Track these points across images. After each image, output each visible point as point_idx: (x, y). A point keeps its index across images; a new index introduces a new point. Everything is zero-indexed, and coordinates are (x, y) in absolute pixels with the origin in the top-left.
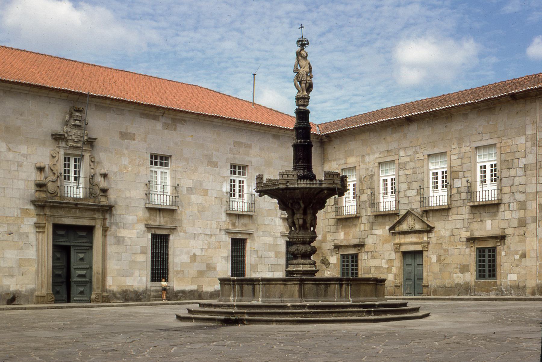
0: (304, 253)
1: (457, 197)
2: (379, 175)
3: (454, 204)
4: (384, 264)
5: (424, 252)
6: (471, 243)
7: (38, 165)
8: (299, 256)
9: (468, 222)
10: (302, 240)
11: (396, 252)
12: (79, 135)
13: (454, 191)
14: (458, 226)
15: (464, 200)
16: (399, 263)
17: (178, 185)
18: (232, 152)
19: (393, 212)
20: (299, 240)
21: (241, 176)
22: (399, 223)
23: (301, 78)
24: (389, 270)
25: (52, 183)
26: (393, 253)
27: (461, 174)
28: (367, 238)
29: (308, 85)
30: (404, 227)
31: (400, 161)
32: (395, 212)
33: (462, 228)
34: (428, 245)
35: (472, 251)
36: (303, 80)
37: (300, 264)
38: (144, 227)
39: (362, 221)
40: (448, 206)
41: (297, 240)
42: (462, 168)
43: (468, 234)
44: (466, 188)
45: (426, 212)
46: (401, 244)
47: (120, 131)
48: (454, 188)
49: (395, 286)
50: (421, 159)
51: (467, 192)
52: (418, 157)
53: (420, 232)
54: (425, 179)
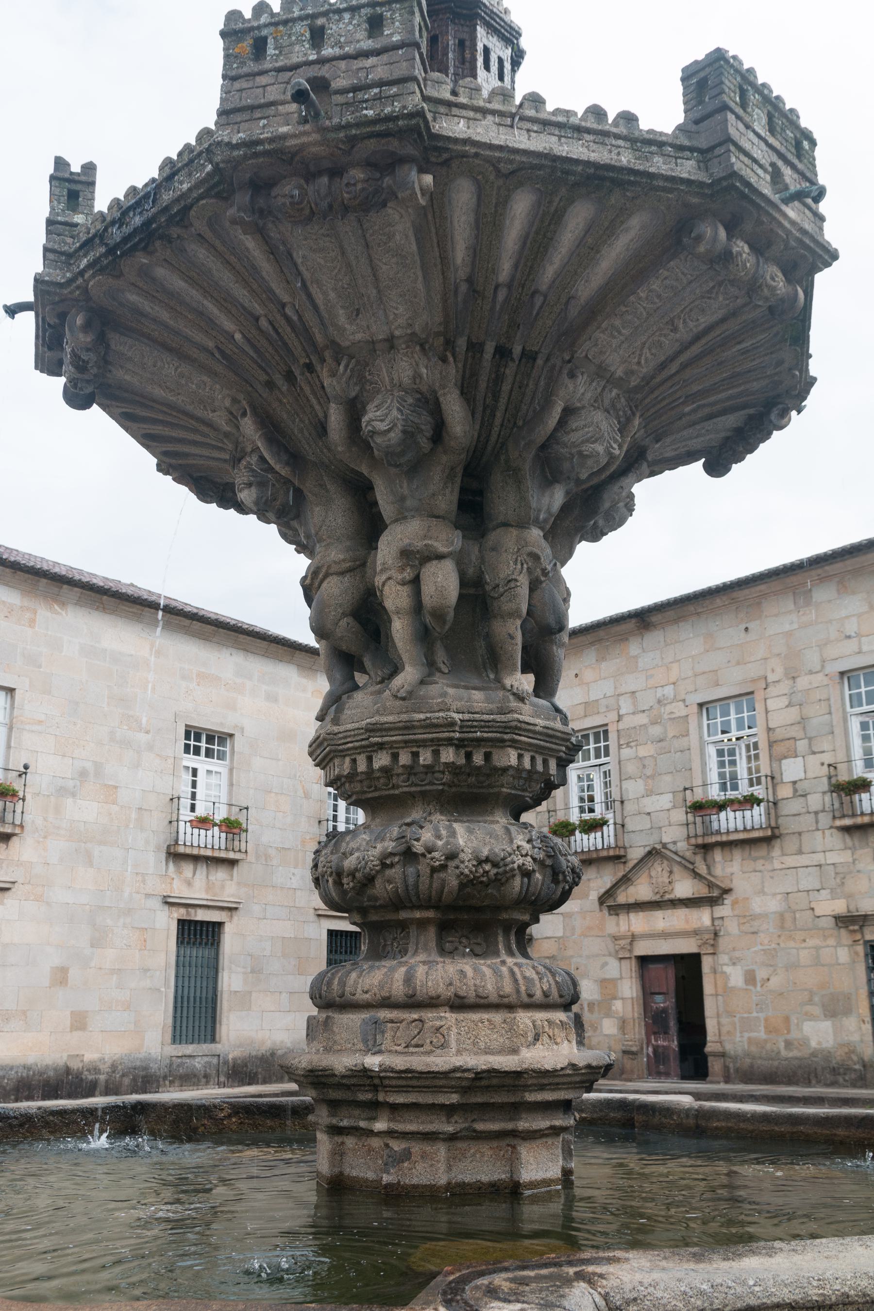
0: (468, 883)
3: (788, 825)
6: (854, 931)
8: (422, 924)
9: (837, 873)
10: (448, 755)
11: (621, 959)
13: (784, 792)
14: (804, 885)
15: (816, 813)
16: (631, 988)
17: (26, 767)
19: (611, 853)
20: (425, 757)
22: (625, 880)
27: (802, 745)
30: (641, 890)
31: (621, 726)
32: (617, 853)
33: (818, 891)
35: (856, 953)
37: (433, 1003)
40: (772, 831)
41: (405, 759)
43: (840, 907)
44: (825, 780)
46: (633, 938)
48: (782, 782)
49: (624, 1052)
50: (680, 717)
51: (824, 793)
52: (672, 713)
54: (696, 765)
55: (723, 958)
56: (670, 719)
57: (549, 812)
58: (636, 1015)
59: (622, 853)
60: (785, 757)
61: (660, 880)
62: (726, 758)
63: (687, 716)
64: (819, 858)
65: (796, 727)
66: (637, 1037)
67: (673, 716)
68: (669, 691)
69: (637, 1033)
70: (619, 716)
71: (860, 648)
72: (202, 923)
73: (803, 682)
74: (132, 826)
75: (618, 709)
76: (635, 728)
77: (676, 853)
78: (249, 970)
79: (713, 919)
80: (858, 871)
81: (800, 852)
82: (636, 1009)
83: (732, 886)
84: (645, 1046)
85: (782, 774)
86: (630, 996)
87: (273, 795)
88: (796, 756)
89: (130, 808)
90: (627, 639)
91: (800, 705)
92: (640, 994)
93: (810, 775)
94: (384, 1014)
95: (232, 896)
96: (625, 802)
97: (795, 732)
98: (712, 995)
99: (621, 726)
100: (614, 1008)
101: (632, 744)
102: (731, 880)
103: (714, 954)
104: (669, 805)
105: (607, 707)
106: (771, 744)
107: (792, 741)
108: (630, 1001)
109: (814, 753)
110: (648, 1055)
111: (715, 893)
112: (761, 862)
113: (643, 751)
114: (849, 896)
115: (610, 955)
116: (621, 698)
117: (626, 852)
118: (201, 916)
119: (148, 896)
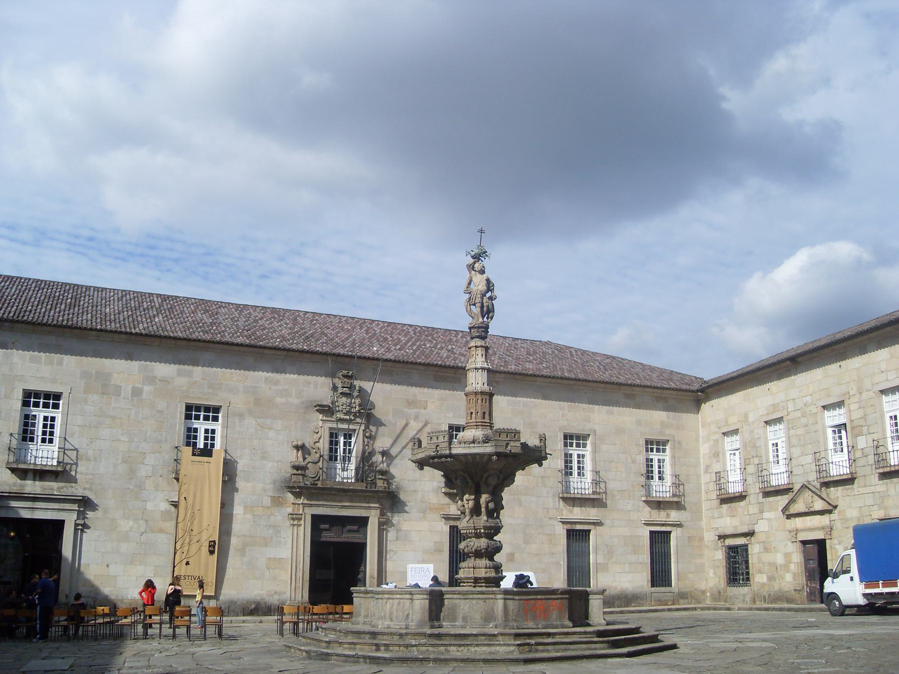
1: (861, 462)
2: (766, 438)
3: (860, 472)
4: (780, 559)
5: (827, 541)
7: (295, 443)
8: (473, 556)
12: (348, 406)
13: (858, 454)
15: (871, 465)
16: (797, 557)
18: (565, 418)
19: (785, 487)
21: (581, 448)
22: (792, 501)
23: (474, 300)
24: (786, 567)
25: (312, 464)
26: (790, 544)
27: (865, 429)
28: (757, 524)
29: (485, 309)
32: (788, 487)
34: (831, 531)
36: (476, 302)
38: (439, 517)
39: (750, 502)
40: (852, 475)
42: (865, 420)
45: (827, 485)
47: (406, 399)
50: (814, 413)
52: (811, 411)
53: (821, 513)
55: (835, 541)
56: (810, 414)
57: (758, 465)
58: (800, 571)
59: (791, 486)
60: (858, 436)
61: (808, 500)
62: (837, 435)
63: (817, 413)
64: (872, 489)
65: (862, 420)
66: (800, 582)
67: (812, 412)
68: (809, 399)
69: (802, 579)
70: (788, 412)
71: (887, 378)
72: (580, 531)
73: (865, 395)
74: (540, 485)
75: (788, 408)
76: (795, 419)
77: (814, 486)
78: (606, 552)
79: (830, 521)
80: (889, 496)
81: (865, 486)
82: (799, 568)
83: (838, 504)
84: (805, 588)
85: (857, 445)
86: (796, 561)
87: (614, 463)
88: (863, 435)
89: (538, 477)
90: (790, 370)
91: (864, 408)
92: (803, 560)
93: (869, 446)
94: (466, 569)
95: (595, 516)
96: (792, 459)
97: (861, 422)
98: (830, 560)
99: (789, 418)
100: (790, 568)
101: (794, 428)
102: (838, 501)
103: (831, 539)
104: (810, 461)
105: (783, 407)
106: (853, 428)
107: (861, 427)
108: (796, 565)
109: (870, 434)
110: (807, 591)
111: (830, 508)
112: (850, 491)
113: (800, 431)
114: (886, 508)
115: (789, 540)
116: (788, 402)
117: (793, 486)
118: (578, 527)
119: (550, 518)
